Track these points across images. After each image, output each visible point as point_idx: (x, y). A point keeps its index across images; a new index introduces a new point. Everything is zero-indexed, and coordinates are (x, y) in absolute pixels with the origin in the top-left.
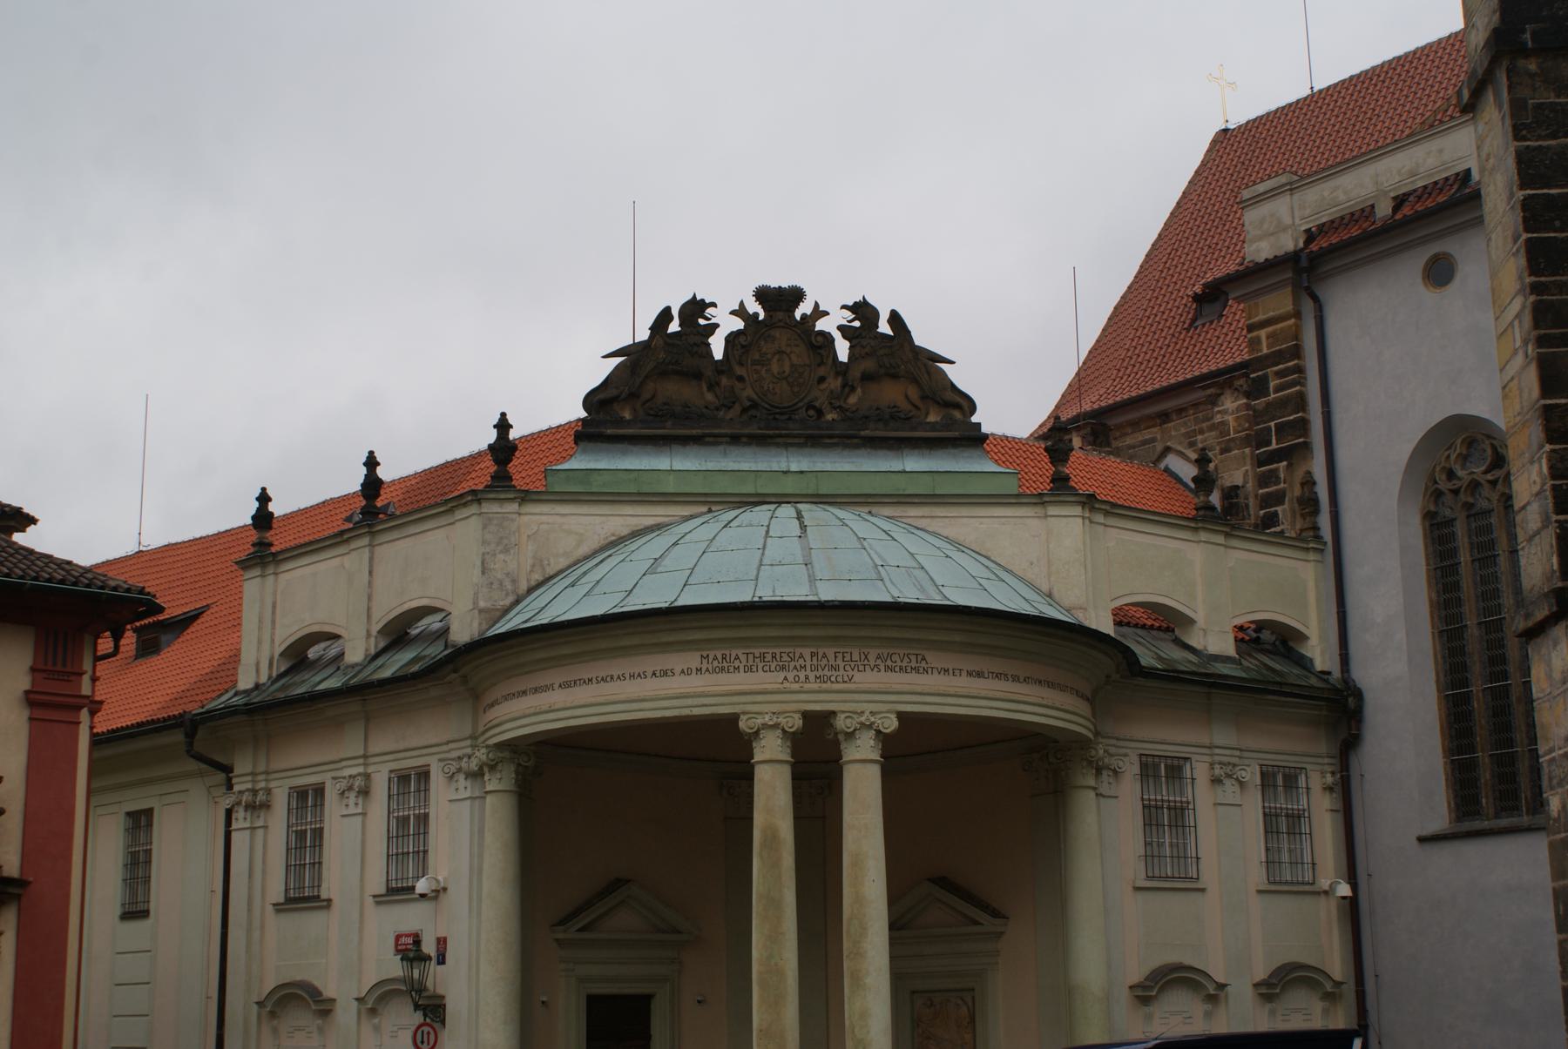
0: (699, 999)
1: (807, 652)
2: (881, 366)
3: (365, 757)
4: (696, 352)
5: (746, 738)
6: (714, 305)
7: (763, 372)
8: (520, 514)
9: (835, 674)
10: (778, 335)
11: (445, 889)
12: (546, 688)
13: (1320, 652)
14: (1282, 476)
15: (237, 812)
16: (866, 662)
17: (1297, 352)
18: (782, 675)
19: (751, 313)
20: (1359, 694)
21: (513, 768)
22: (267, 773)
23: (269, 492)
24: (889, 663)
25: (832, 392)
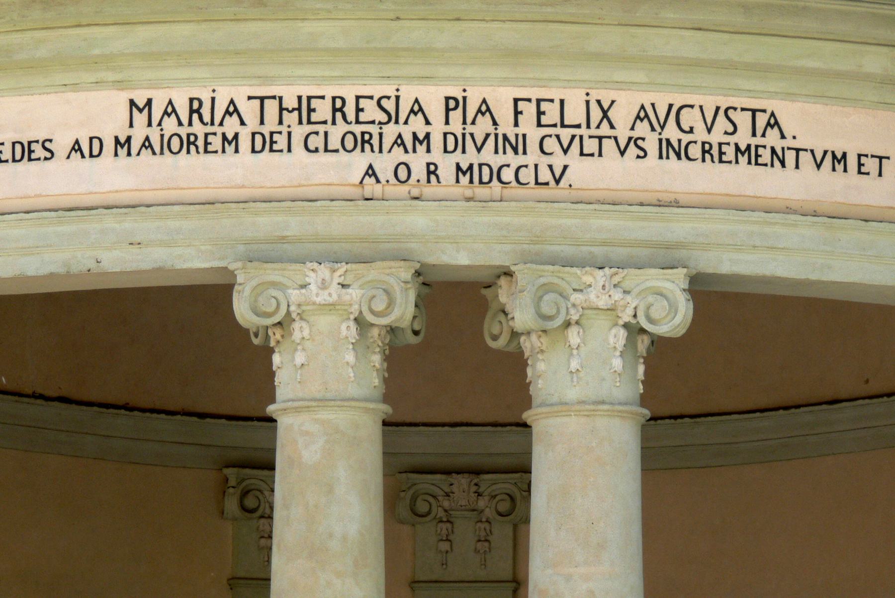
5: (256, 341)
9: (520, 160)
16: (605, 130)
18: (360, 161)
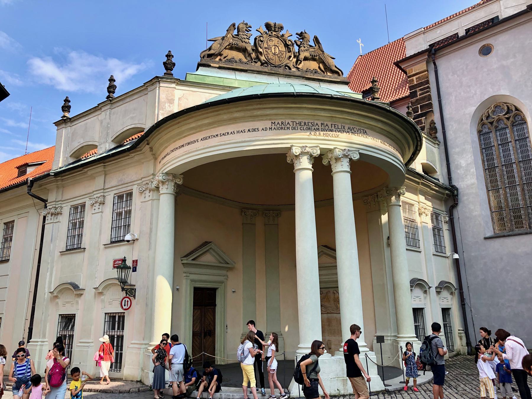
2: (310, 55)
3: (104, 189)
10: (274, 40)
11: (137, 239)
12: (195, 142)
13: (441, 176)
16: (344, 130)
17: (427, 82)
20: (457, 189)
21: (173, 184)
24: (353, 131)
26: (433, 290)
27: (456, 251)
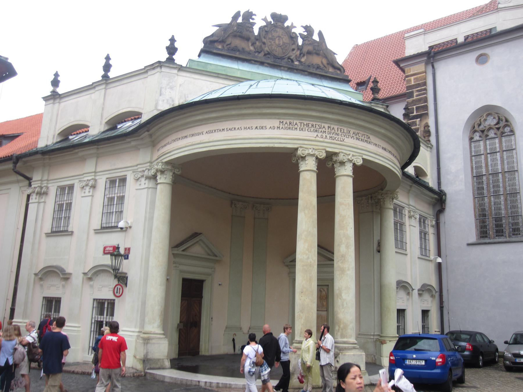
0: (220, 283)
1: (326, 126)
2: (314, 49)
3: (95, 172)
4: (249, 30)
6: (255, 15)
7: (273, 42)
8: (177, 75)
9: (338, 137)
11: (130, 227)
12: (199, 134)
13: (431, 180)
14: (418, 123)
15: (32, 196)
16: (349, 134)
17: (425, 84)
18: (316, 134)
19: (269, 21)
21: (171, 174)
22: (48, 180)
23: (59, 73)
24: (357, 136)
25: (296, 55)
26: (416, 292)
27: (439, 255)
